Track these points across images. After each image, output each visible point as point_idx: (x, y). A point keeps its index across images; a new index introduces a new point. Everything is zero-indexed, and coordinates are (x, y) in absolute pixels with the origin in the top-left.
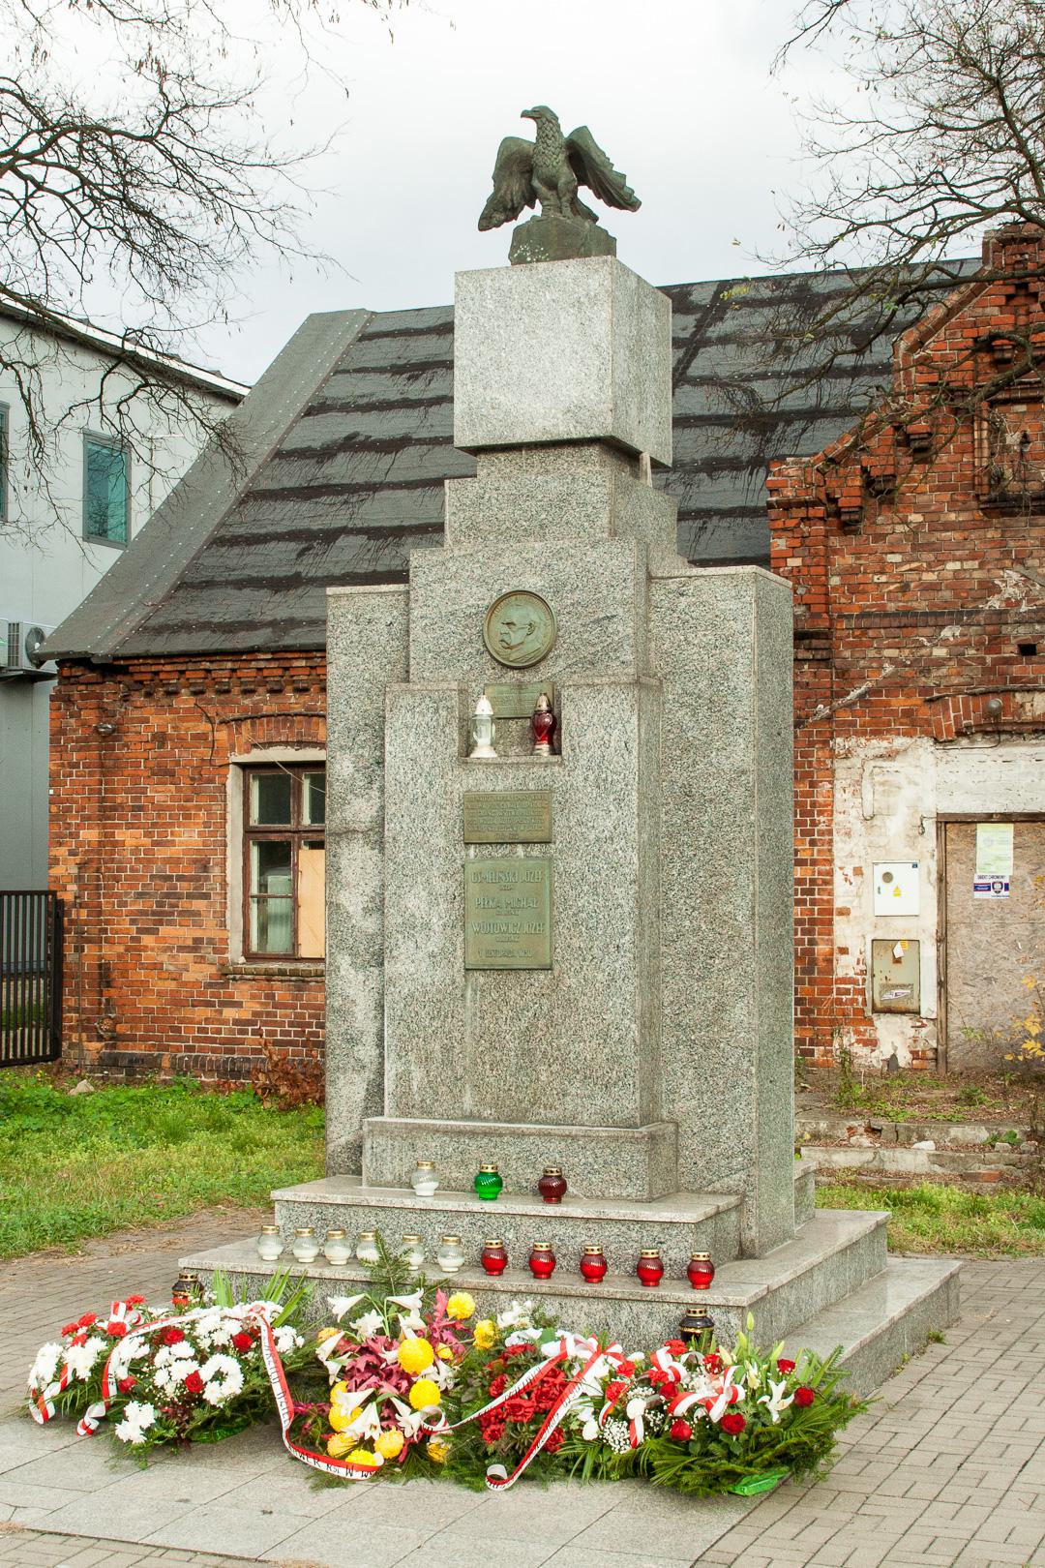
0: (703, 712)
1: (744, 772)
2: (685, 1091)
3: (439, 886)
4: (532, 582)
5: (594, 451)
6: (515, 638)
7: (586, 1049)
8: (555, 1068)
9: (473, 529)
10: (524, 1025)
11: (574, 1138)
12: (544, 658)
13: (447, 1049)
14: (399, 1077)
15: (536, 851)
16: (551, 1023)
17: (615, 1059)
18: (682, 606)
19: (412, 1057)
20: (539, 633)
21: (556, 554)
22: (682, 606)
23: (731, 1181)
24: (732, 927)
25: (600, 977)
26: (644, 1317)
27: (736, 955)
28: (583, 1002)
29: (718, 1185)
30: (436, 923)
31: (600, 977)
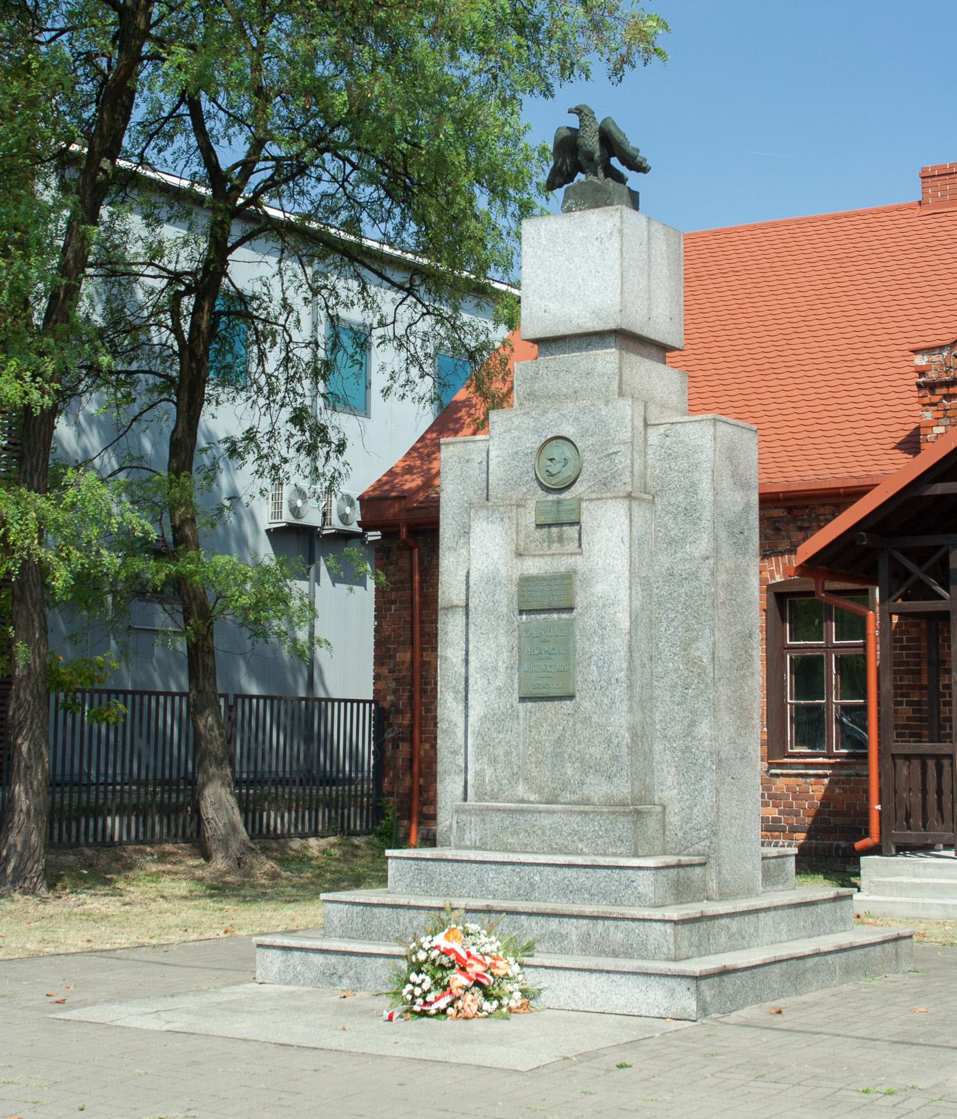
0: (681, 517)
1: (707, 558)
2: (669, 783)
3: (503, 640)
4: (568, 430)
5: (612, 339)
6: (554, 470)
7: (596, 751)
8: (577, 765)
9: (532, 396)
10: (557, 735)
11: (586, 813)
12: (574, 482)
13: (507, 754)
14: (477, 773)
15: (564, 616)
16: (575, 733)
17: (615, 758)
18: (667, 444)
19: (485, 759)
20: (571, 465)
21: (583, 410)
22: (667, 444)
23: (699, 847)
24: (700, 666)
25: (605, 700)
26: (612, 929)
27: (702, 686)
28: (595, 718)
29: (691, 850)
30: (502, 666)
31: (605, 700)
